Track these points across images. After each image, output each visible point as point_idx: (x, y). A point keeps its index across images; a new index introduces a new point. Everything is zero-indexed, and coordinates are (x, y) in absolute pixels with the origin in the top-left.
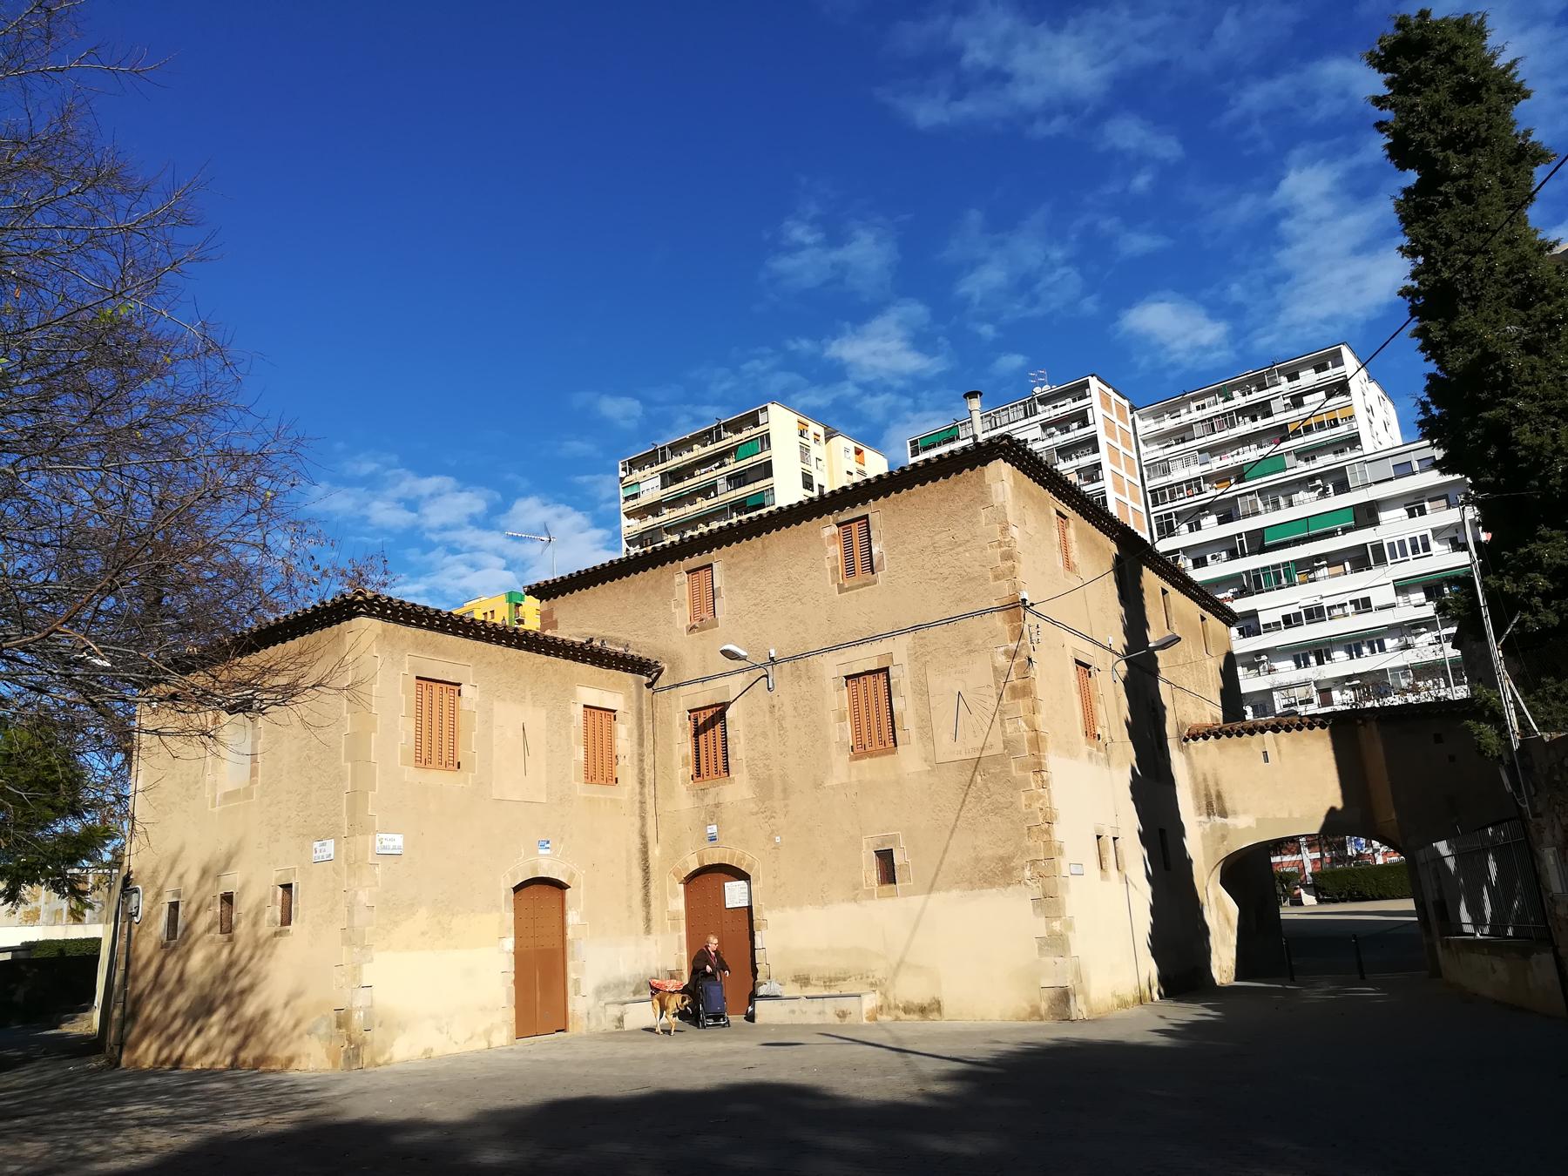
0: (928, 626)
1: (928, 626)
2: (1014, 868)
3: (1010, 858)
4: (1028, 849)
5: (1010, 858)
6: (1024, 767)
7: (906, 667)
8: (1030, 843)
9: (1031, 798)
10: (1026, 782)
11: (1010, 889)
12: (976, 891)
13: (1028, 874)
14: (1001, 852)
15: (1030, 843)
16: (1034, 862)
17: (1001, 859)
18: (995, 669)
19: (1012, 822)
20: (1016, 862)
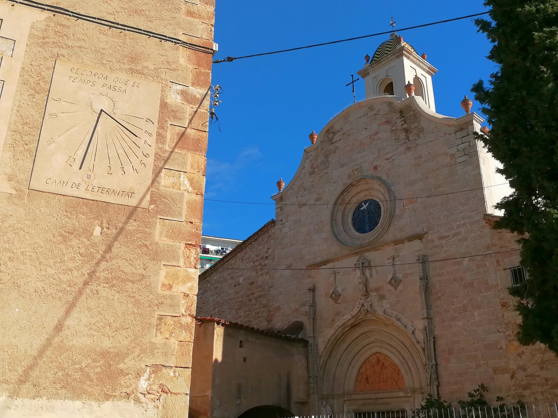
0: (79, 16)
1: (79, 16)
2: (122, 373)
3: (120, 356)
4: (153, 347)
5: (120, 356)
6: (174, 234)
7: (21, 48)
8: (159, 339)
9: (175, 277)
10: (172, 254)
11: (108, 404)
12: (43, 401)
13: (143, 384)
14: (107, 344)
15: (159, 339)
16: (157, 368)
17: (105, 354)
18: (164, 105)
19: (137, 303)
20: (129, 364)
